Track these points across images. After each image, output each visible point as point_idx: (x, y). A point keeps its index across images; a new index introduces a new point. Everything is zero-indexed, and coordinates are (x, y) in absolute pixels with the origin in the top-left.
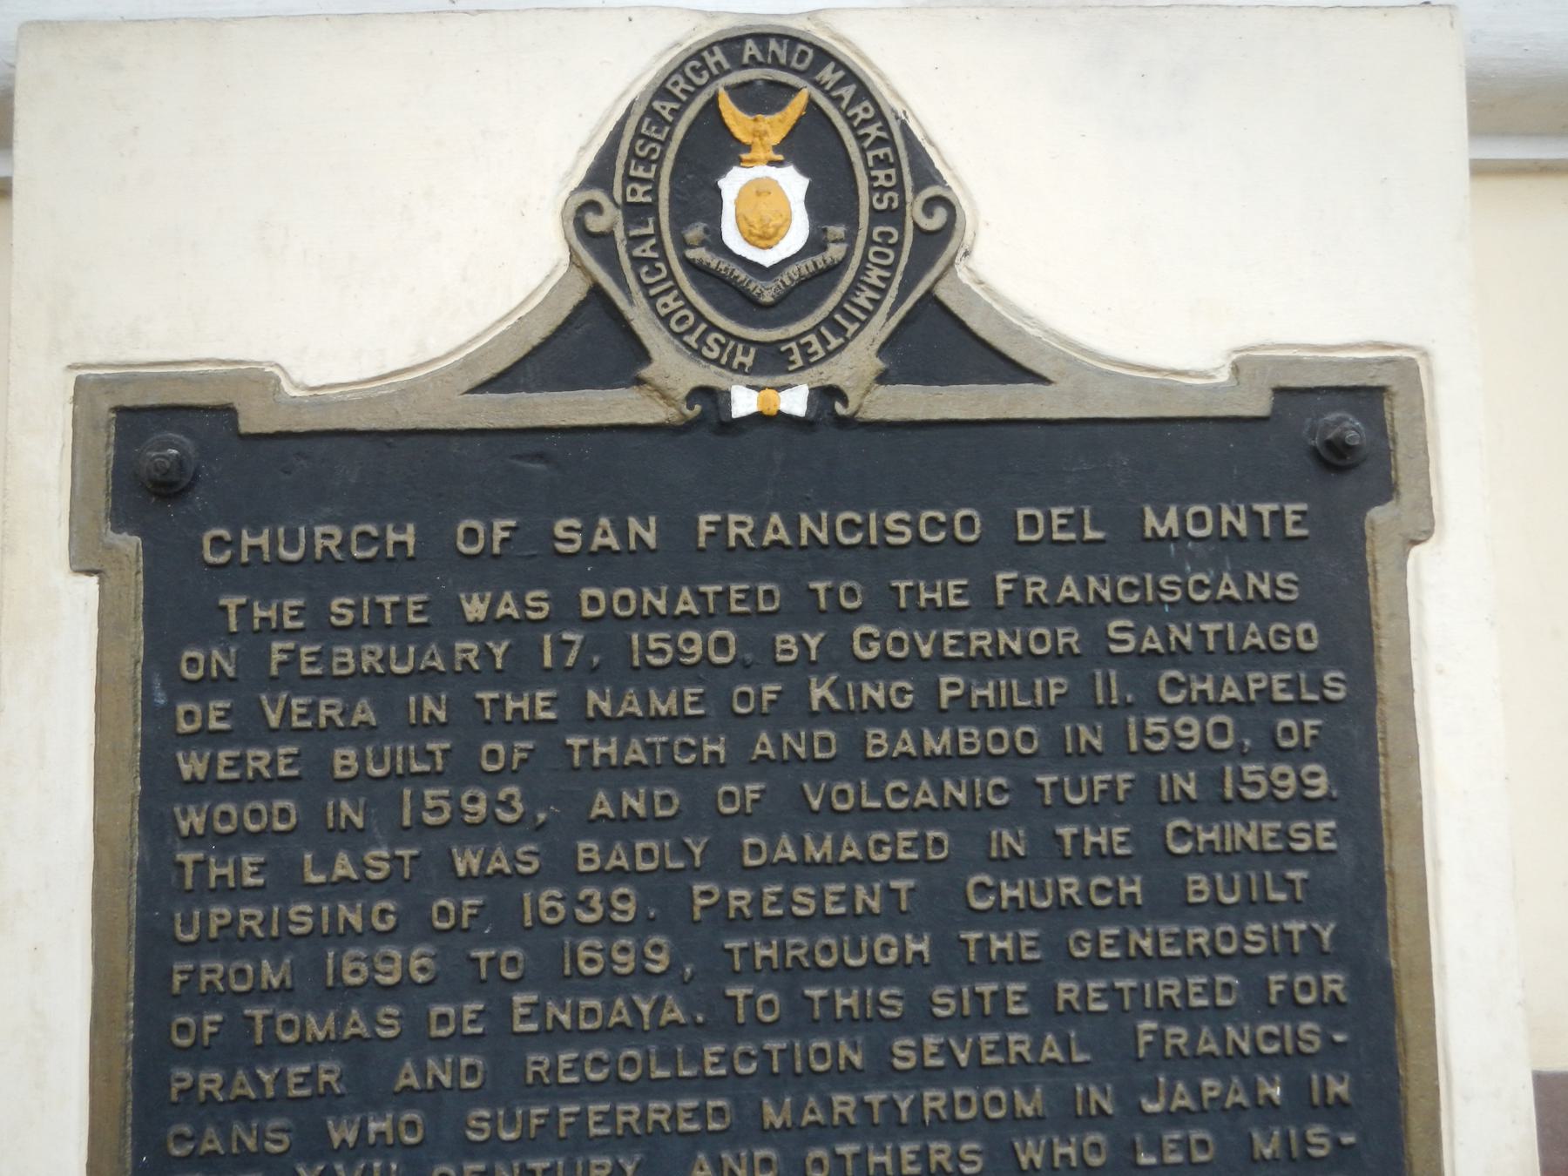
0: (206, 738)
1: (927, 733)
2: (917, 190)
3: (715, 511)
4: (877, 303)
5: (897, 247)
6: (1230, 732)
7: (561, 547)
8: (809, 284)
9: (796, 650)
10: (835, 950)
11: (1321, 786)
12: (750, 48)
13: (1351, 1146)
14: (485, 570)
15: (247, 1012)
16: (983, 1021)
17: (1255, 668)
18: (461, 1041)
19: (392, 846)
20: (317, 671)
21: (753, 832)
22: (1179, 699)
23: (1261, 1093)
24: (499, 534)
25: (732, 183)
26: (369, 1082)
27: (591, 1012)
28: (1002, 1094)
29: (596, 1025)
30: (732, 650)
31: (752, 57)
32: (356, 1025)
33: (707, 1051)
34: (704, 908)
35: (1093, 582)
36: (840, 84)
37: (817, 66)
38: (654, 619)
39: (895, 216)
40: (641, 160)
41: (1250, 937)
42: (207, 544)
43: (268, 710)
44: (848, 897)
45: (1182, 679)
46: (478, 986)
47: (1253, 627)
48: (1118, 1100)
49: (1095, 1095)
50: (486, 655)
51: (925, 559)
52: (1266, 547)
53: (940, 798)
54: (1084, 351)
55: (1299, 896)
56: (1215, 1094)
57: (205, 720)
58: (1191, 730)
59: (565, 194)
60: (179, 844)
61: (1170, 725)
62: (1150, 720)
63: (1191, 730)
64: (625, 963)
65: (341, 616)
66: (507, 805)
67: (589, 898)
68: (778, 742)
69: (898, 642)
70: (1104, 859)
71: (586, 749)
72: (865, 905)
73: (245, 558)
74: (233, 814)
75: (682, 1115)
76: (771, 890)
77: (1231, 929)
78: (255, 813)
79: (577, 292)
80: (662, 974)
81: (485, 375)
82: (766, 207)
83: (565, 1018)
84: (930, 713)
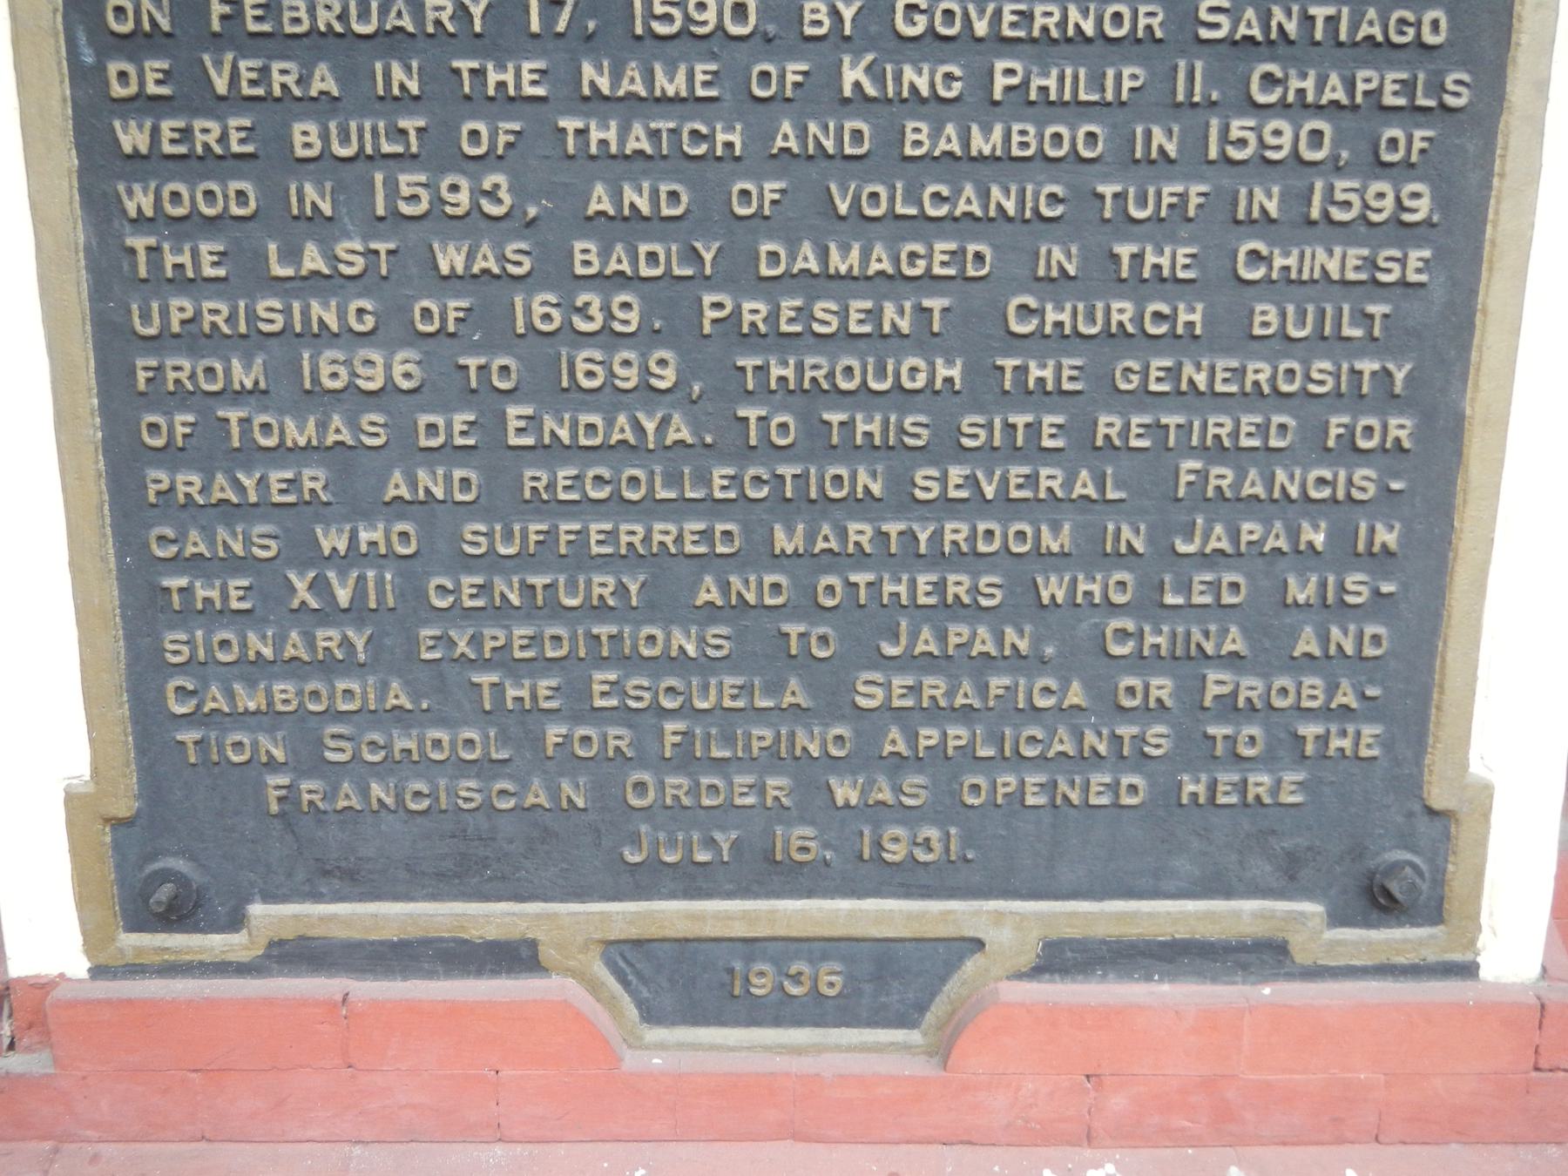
0: (144, 105)
1: (975, 129)
6: (1327, 140)
9: (827, 22)
10: (857, 372)
11: (1422, 209)
13: (1391, 594)
15: (220, 413)
16: (1015, 453)
17: (1366, 64)
18: (451, 453)
19: (365, 238)
21: (771, 237)
22: (1272, 98)
23: (1304, 538)
27: (591, 427)
28: (1028, 529)
29: (597, 441)
30: (752, 19)
32: (339, 431)
33: (716, 474)
34: (715, 321)
41: (1316, 376)
43: (212, 72)
44: (875, 315)
45: (1279, 74)
47: (1372, 13)
48: (1150, 541)
49: (1127, 533)
55: (1377, 332)
56: (1254, 537)
57: (142, 83)
58: (1282, 136)
60: (128, 228)
62: (1236, 123)
63: (1282, 136)
64: (629, 378)
66: (492, 195)
67: (587, 304)
71: (582, 133)
72: (894, 325)
75: (688, 538)
76: (788, 305)
77: (1296, 366)
78: (209, 194)
80: (668, 391)
83: (564, 434)
84: (983, 105)
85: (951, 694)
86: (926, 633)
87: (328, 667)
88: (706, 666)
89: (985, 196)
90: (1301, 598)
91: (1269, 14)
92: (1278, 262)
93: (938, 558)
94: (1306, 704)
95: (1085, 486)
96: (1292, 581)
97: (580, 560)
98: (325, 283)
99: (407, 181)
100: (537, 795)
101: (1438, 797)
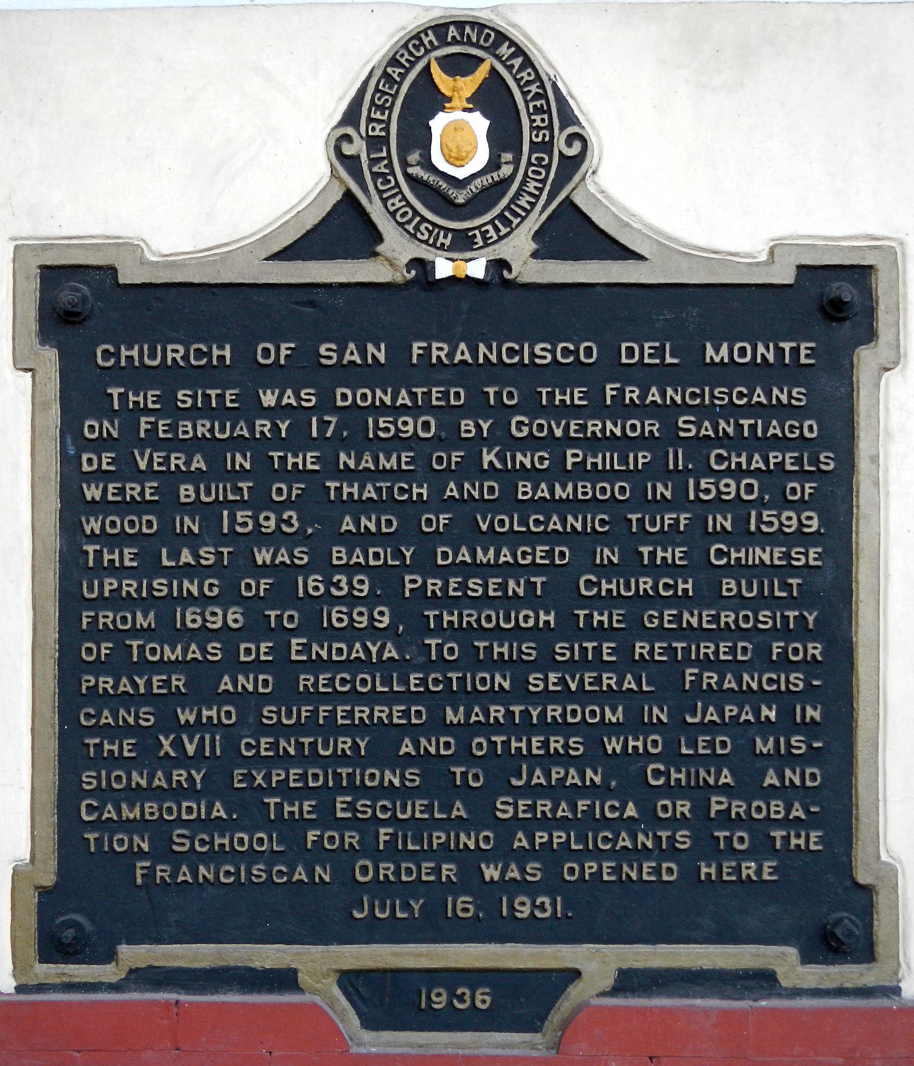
0: (100, 476)
2: (562, 129)
3: (423, 340)
4: (533, 205)
5: (548, 168)
7: (323, 361)
9: (474, 431)
12: (452, 32)
14: (277, 376)
17: (774, 450)
18: (258, 665)
19: (215, 546)
20: (169, 436)
22: (723, 467)
24: (284, 352)
25: (439, 123)
26: (202, 687)
29: (344, 658)
30: (433, 430)
31: (454, 37)
32: (194, 652)
33: (412, 677)
35: (670, 392)
36: (513, 56)
37: (497, 45)
38: (382, 409)
39: (547, 147)
40: (377, 107)
41: (761, 618)
42: (99, 354)
44: (503, 587)
46: (268, 632)
50: (275, 428)
51: (560, 374)
52: (785, 371)
53: (564, 526)
54: (670, 238)
57: (100, 464)
58: (730, 488)
59: (328, 130)
60: (84, 540)
61: (716, 485)
63: (730, 488)
65: (184, 402)
67: (339, 581)
68: (461, 489)
69: (541, 427)
70: (669, 568)
71: (339, 490)
72: (514, 591)
73: (123, 364)
74: (117, 523)
76: (453, 582)
78: (132, 523)
79: (336, 195)
81: (276, 248)
82: (461, 139)
83: (324, 654)
84: (559, 472)
85: (554, 810)
86: (538, 772)
87: (178, 793)
88: (404, 793)
89: (564, 522)
90: (765, 751)
91: (718, 424)
92: (734, 555)
93: (547, 727)
94: (773, 816)
95: (630, 683)
96: (758, 741)
97: (332, 729)
98: (188, 571)
99: (240, 516)
100: (300, 874)
101: (862, 878)
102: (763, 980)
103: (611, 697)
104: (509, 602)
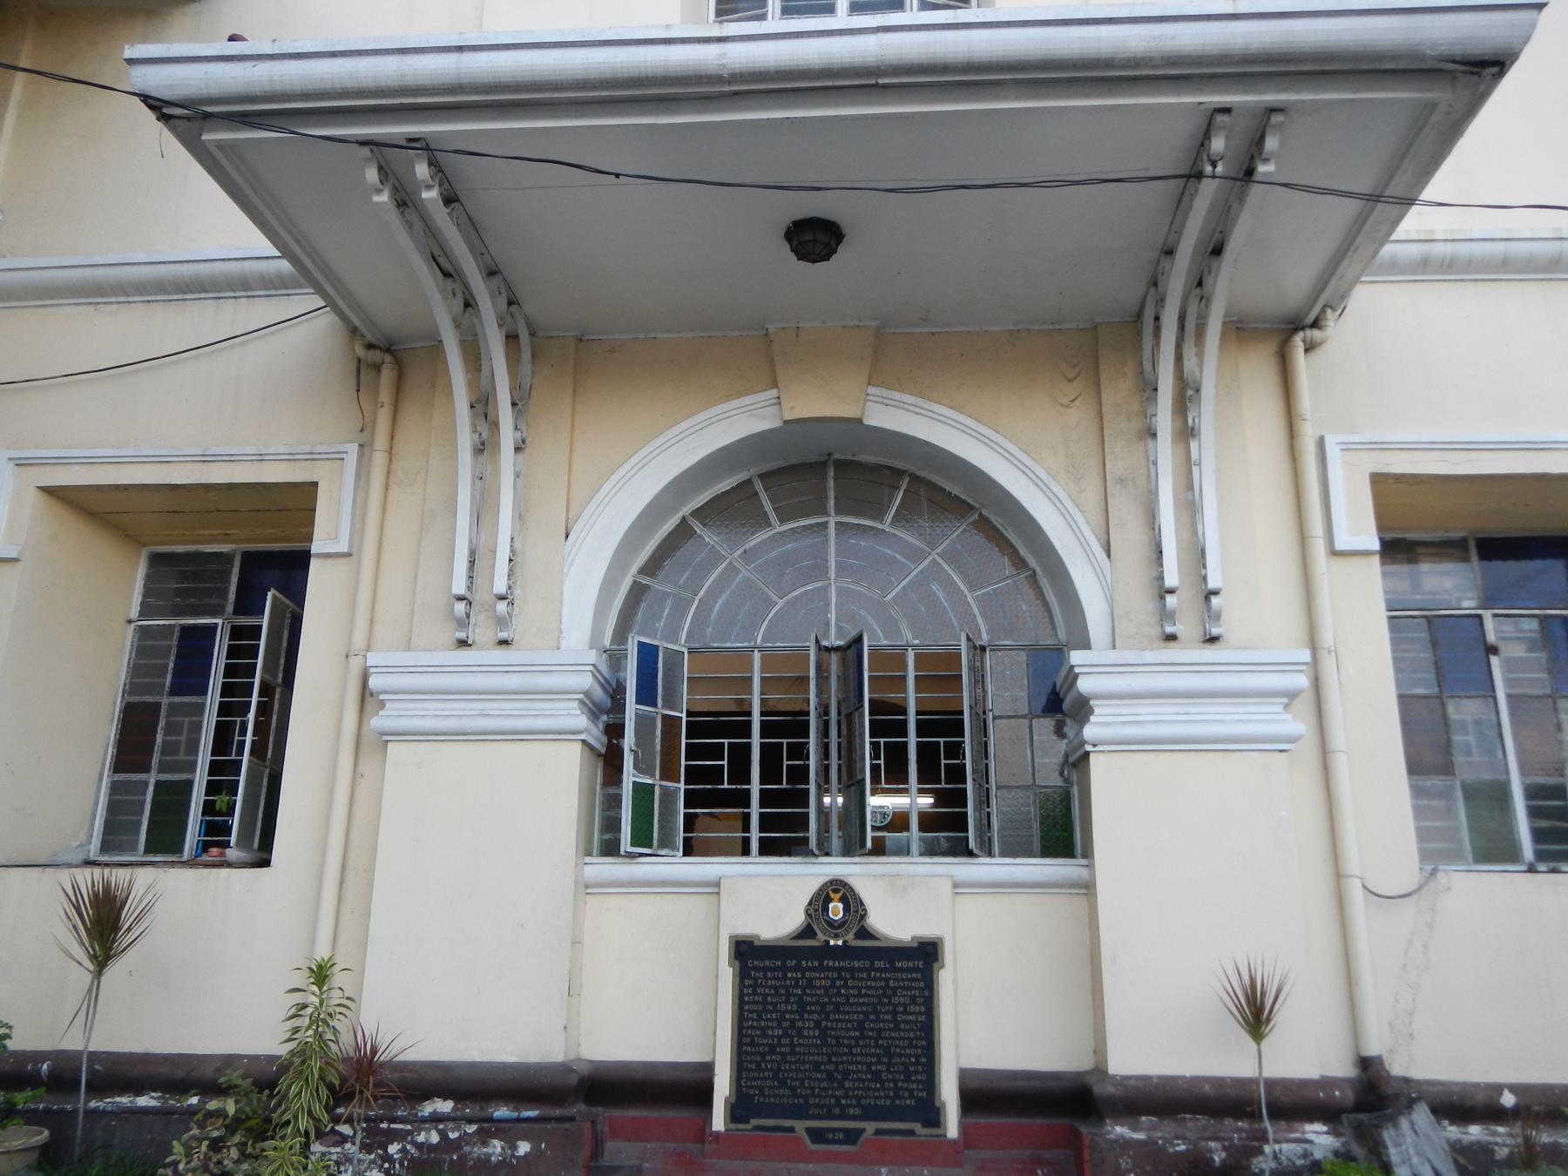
8: (842, 923)
14: (792, 969)
51: (860, 970)
82: (836, 910)
84: (860, 995)
87: (766, 1079)
88: (821, 1080)
93: (858, 1063)
97: (804, 1062)
98: (771, 1020)
102: (911, 1133)
103: (873, 1055)
104: (848, 1030)
